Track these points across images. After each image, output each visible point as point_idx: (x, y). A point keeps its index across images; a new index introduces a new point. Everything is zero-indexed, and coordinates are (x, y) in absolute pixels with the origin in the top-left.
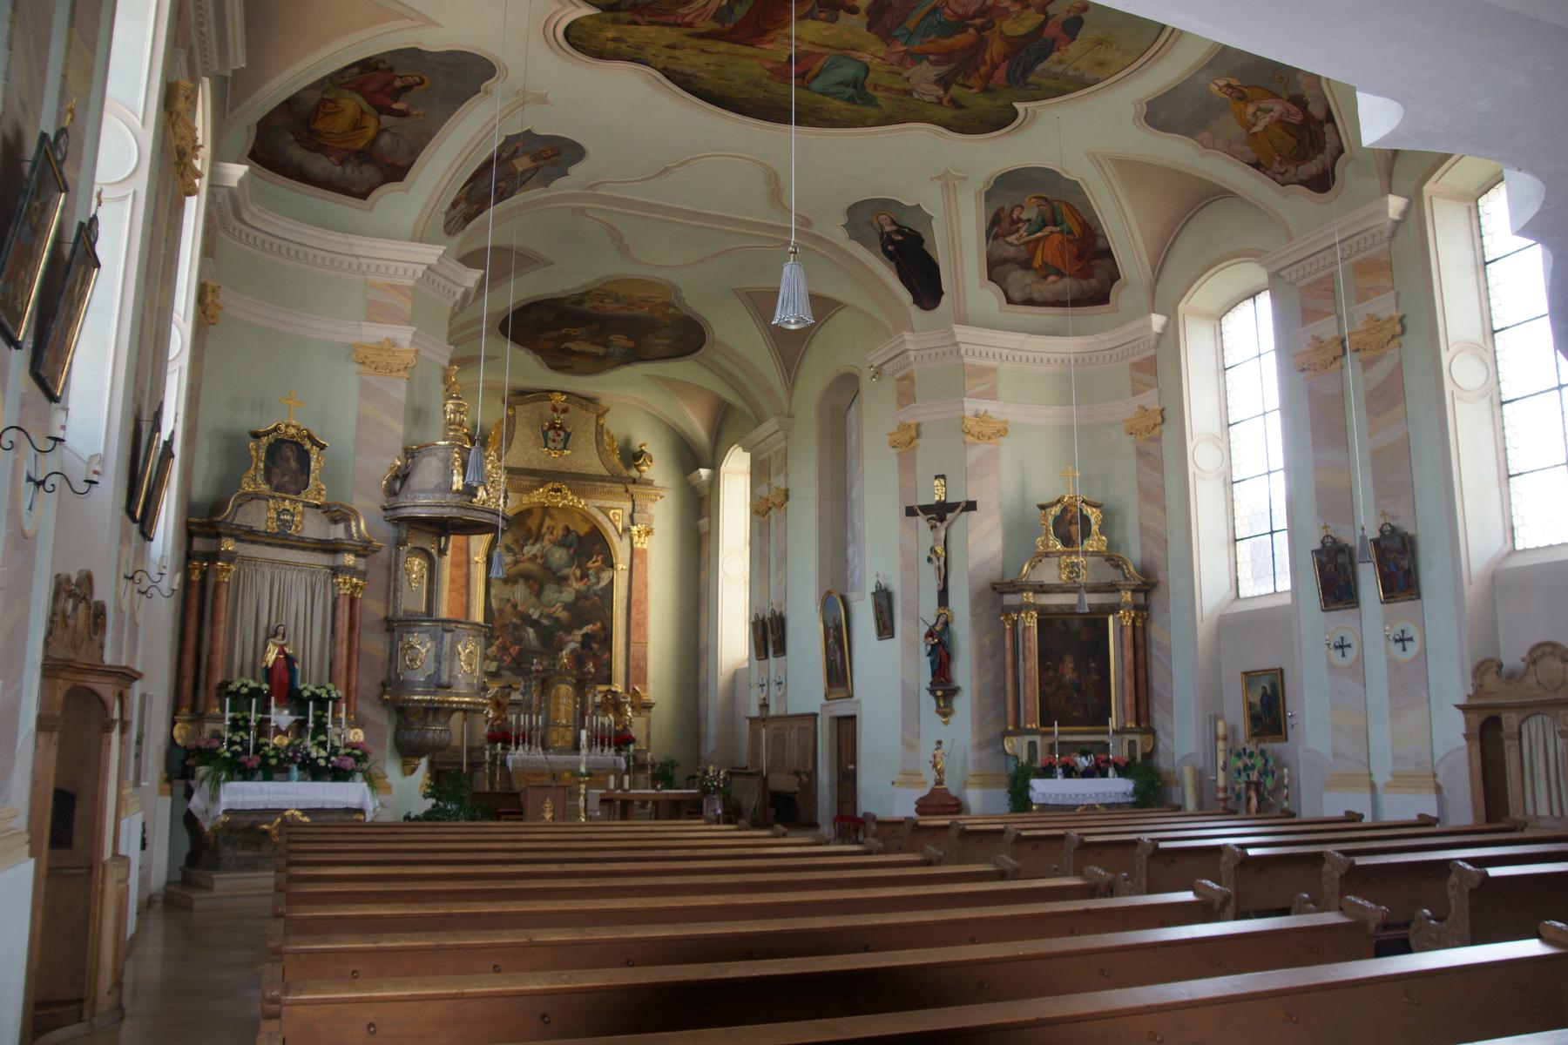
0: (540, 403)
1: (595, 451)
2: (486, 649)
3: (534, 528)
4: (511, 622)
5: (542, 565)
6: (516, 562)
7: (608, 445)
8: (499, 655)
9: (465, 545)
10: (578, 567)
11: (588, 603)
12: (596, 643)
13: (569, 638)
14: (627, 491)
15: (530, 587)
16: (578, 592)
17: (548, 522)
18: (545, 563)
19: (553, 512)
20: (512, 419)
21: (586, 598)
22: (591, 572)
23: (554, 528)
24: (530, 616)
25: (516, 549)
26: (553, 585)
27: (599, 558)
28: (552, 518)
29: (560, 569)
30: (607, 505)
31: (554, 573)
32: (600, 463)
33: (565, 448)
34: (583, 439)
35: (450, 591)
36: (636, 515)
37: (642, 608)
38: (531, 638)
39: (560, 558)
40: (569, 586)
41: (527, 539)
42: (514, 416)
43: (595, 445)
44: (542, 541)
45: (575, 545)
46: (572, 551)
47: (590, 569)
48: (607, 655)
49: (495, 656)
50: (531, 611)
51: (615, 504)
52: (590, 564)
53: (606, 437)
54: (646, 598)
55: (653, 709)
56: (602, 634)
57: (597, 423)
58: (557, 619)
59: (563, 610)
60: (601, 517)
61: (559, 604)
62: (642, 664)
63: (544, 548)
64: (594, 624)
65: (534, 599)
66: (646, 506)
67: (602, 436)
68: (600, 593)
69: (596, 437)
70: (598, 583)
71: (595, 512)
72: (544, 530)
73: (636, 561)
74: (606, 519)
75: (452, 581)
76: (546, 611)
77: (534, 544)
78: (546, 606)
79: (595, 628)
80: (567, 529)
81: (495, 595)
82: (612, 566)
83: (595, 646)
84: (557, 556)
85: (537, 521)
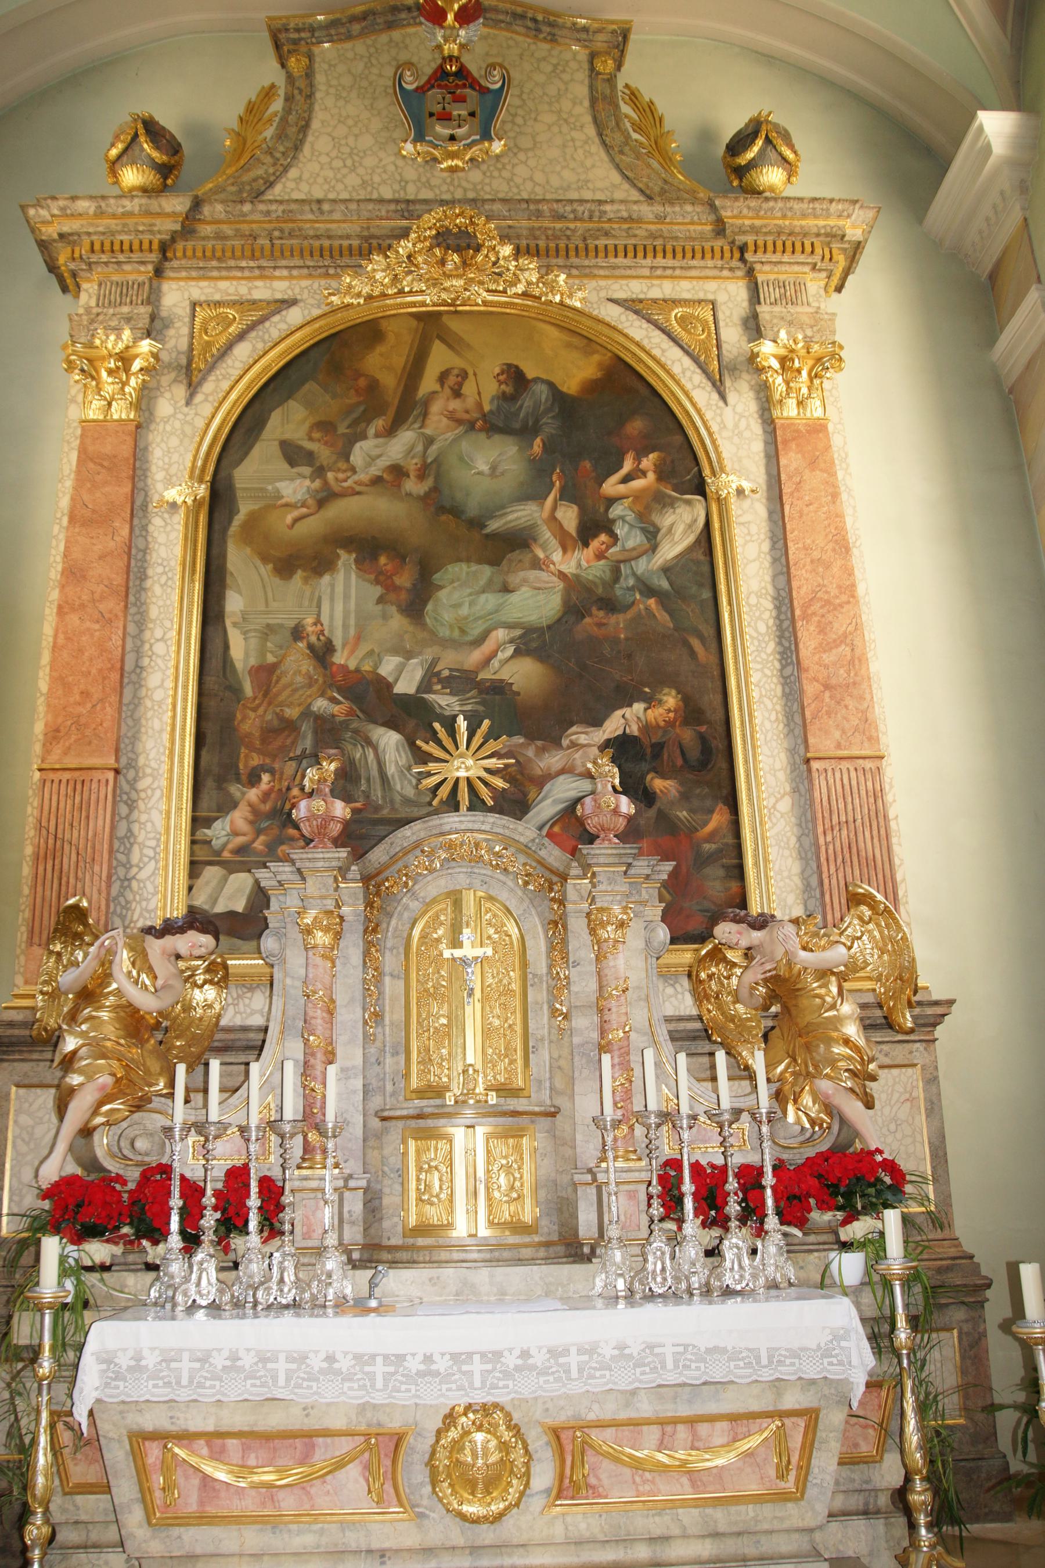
0: (396, 34)
1: (596, 148)
2: (198, 822)
3: (390, 382)
4: (307, 713)
5: (425, 498)
6: (325, 498)
7: (638, 128)
8: (258, 845)
9: (126, 450)
10: (568, 495)
11: (618, 622)
12: (664, 776)
13: (554, 760)
14: (720, 228)
15: (382, 579)
16: (572, 584)
17: (439, 358)
18: (435, 489)
19: (454, 325)
20: (301, 83)
21: (610, 605)
22: (616, 511)
23: (464, 375)
24: (383, 686)
25: (324, 453)
26: (474, 567)
27: (648, 462)
28: (452, 342)
29: (491, 513)
30: (655, 293)
31: (477, 524)
32: (616, 177)
33: (486, 136)
34: (548, 118)
35: (61, 611)
36: (763, 310)
37: (840, 625)
38: (391, 770)
39: (493, 468)
40: (536, 564)
41: (367, 418)
42: (309, 74)
43: (591, 131)
44: (425, 414)
45: (550, 426)
46: (538, 442)
47: (611, 501)
48: (718, 819)
49: (241, 850)
50: (387, 668)
51: (685, 289)
52: (611, 486)
53: (626, 109)
54: (850, 590)
55: (939, 1031)
56: (687, 735)
57: (592, 69)
58: (499, 688)
59: (517, 653)
60: (637, 329)
61: (501, 634)
62: (867, 844)
63: (429, 441)
64: (650, 701)
65: (398, 622)
66: (799, 286)
67: (617, 106)
68: (665, 584)
69: (593, 101)
70: (654, 548)
71: (612, 314)
72: (428, 383)
73: (790, 460)
74: (657, 337)
75: (73, 573)
76: (449, 661)
77: (390, 431)
78: (447, 643)
79: (657, 714)
80: (516, 377)
81: (245, 616)
82: (700, 488)
83: (658, 784)
84: (484, 468)
85: (400, 360)
